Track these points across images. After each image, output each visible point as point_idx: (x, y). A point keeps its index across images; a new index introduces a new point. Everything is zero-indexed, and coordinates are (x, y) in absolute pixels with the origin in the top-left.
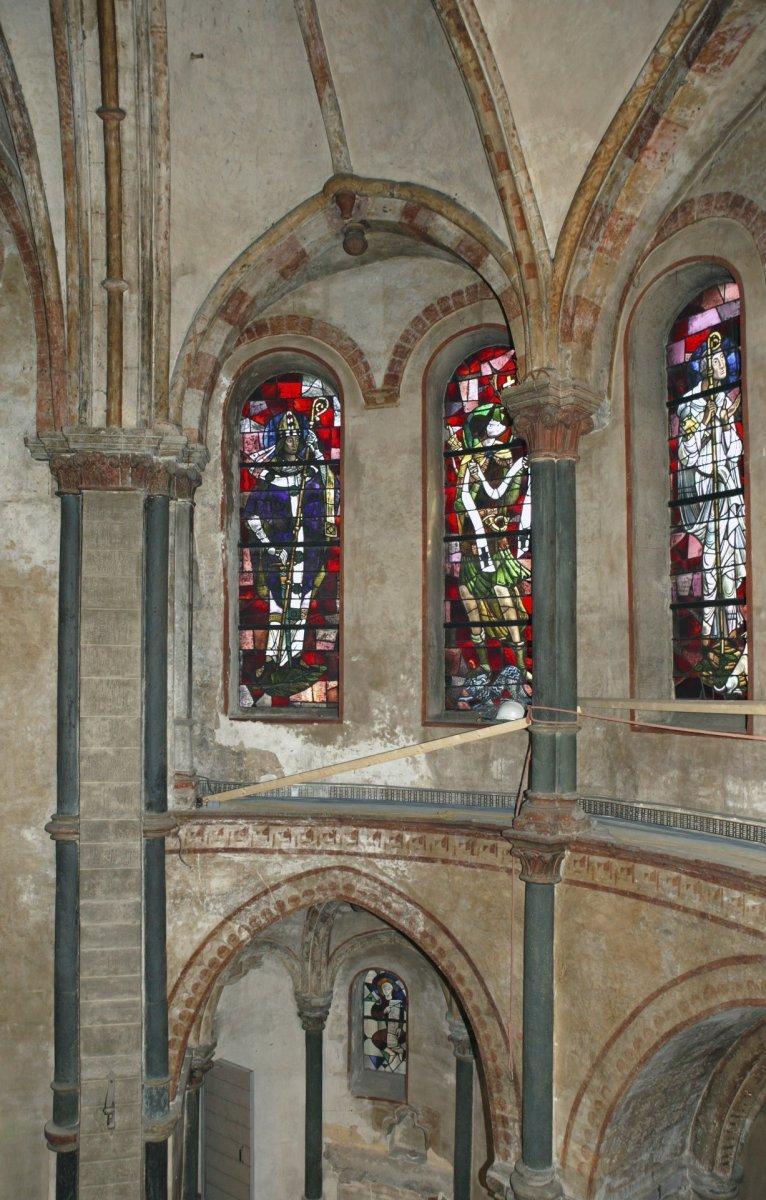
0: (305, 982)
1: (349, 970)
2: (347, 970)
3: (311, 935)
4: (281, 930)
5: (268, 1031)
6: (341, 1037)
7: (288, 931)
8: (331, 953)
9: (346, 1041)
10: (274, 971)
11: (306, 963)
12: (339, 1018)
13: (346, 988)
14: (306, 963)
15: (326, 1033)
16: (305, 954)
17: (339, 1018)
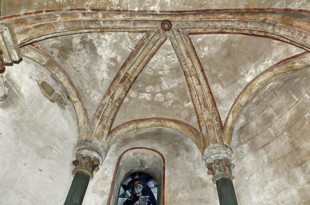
0: (90, 132)
1: (121, 147)
2: (119, 147)
3: (108, 97)
4: (88, 91)
5: (44, 158)
6: (103, 193)
7: (91, 95)
8: (112, 128)
9: (106, 197)
10: (69, 121)
11: (96, 120)
12: (105, 178)
13: (116, 159)
14: (96, 120)
15: (91, 184)
16: (98, 113)
17: (105, 178)
